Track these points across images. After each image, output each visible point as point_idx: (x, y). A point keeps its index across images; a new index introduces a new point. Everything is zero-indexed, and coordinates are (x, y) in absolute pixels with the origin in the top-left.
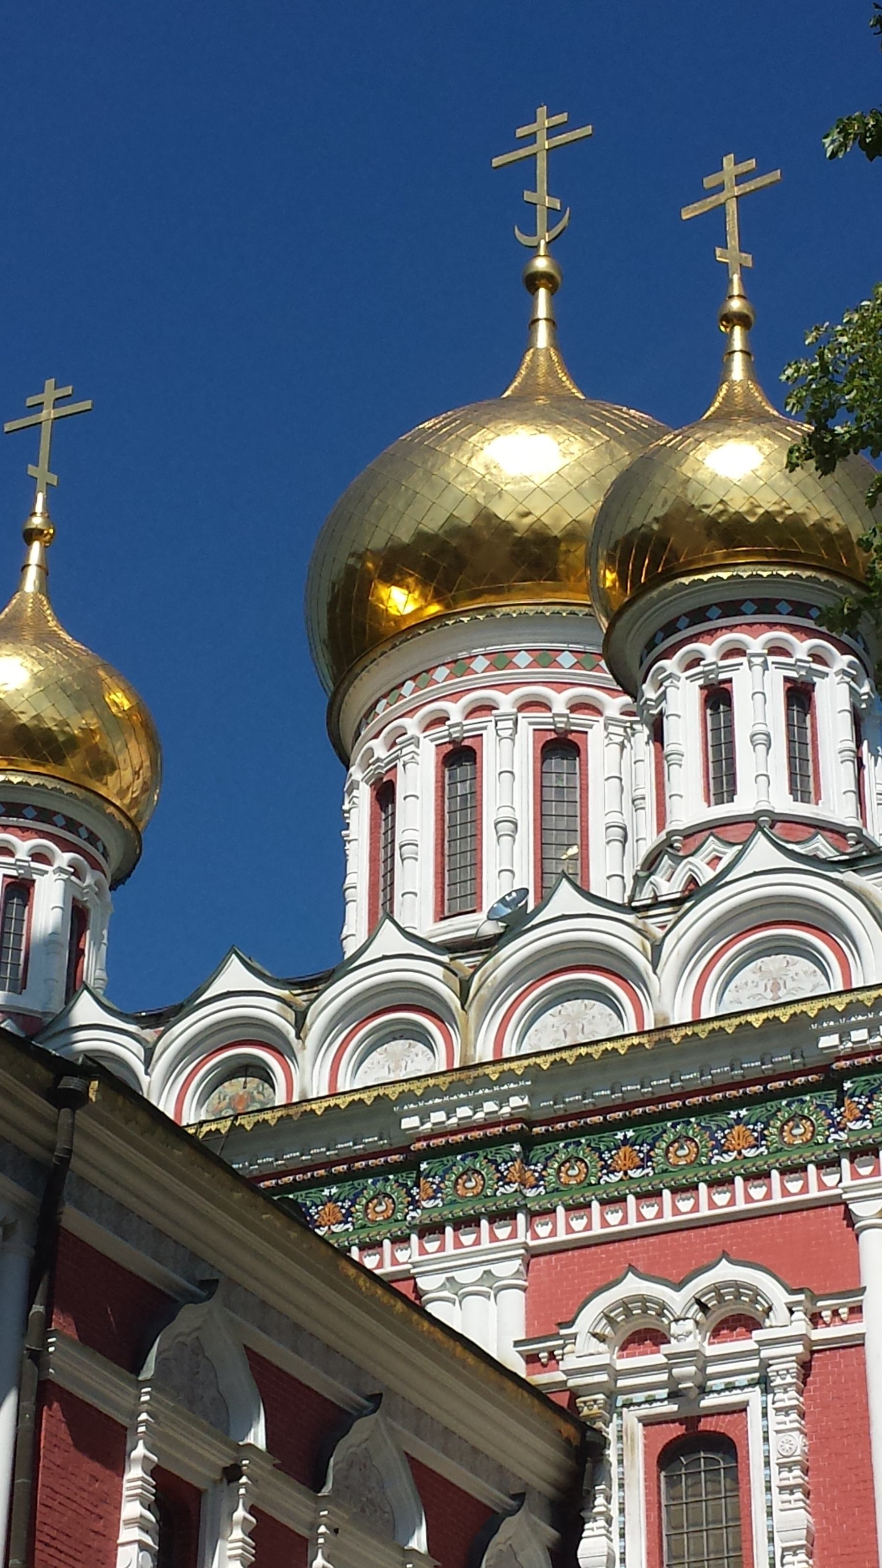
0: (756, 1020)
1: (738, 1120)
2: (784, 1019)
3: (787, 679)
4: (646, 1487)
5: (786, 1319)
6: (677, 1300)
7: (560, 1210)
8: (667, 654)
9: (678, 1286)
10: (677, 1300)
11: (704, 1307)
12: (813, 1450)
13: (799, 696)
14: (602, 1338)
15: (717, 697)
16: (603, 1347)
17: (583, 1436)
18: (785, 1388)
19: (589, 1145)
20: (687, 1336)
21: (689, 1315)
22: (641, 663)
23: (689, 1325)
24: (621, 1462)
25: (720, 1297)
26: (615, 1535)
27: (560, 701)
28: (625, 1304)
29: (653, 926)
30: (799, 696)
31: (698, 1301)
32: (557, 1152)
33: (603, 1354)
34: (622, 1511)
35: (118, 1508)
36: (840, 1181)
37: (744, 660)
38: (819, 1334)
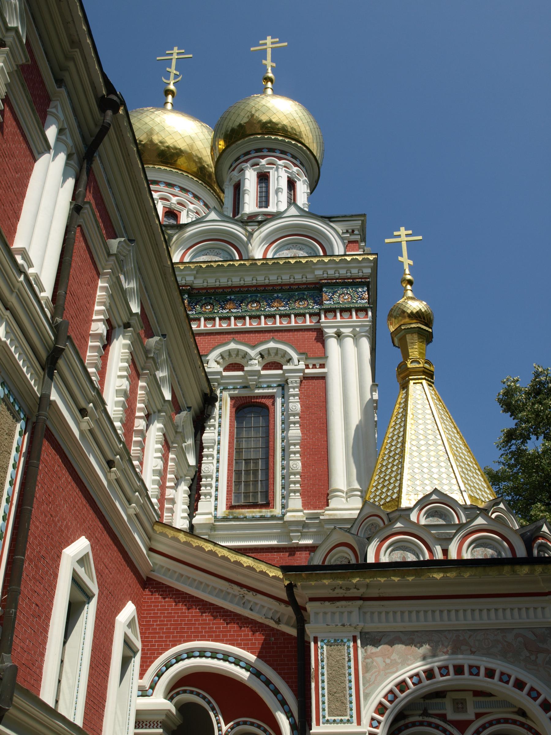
0: (292, 261)
1: (278, 297)
2: (304, 262)
3: (288, 177)
4: (230, 419)
5: (297, 364)
6: (253, 353)
7: (202, 319)
8: (246, 161)
9: (253, 347)
10: (253, 353)
11: (262, 356)
12: (302, 411)
13: (291, 184)
14: (218, 363)
15: (263, 178)
16: (219, 366)
17: (211, 394)
18: (294, 388)
19: (215, 299)
20: (255, 365)
21: (257, 358)
22: (231, 166)
23: (256, 362)
24: (220, 409)
25: (269, 353)
26: (217, 434)
27: (174, 200)
28: (229, 352)
29: (249, 229)
30: (291, 184)
31: (260, 354)
32: (201, 300)
33: (219, 368)
34: (220, 426)
35: (94, 304)
36: (320, 319)
37: (275, 166)
38: (307, 371)
